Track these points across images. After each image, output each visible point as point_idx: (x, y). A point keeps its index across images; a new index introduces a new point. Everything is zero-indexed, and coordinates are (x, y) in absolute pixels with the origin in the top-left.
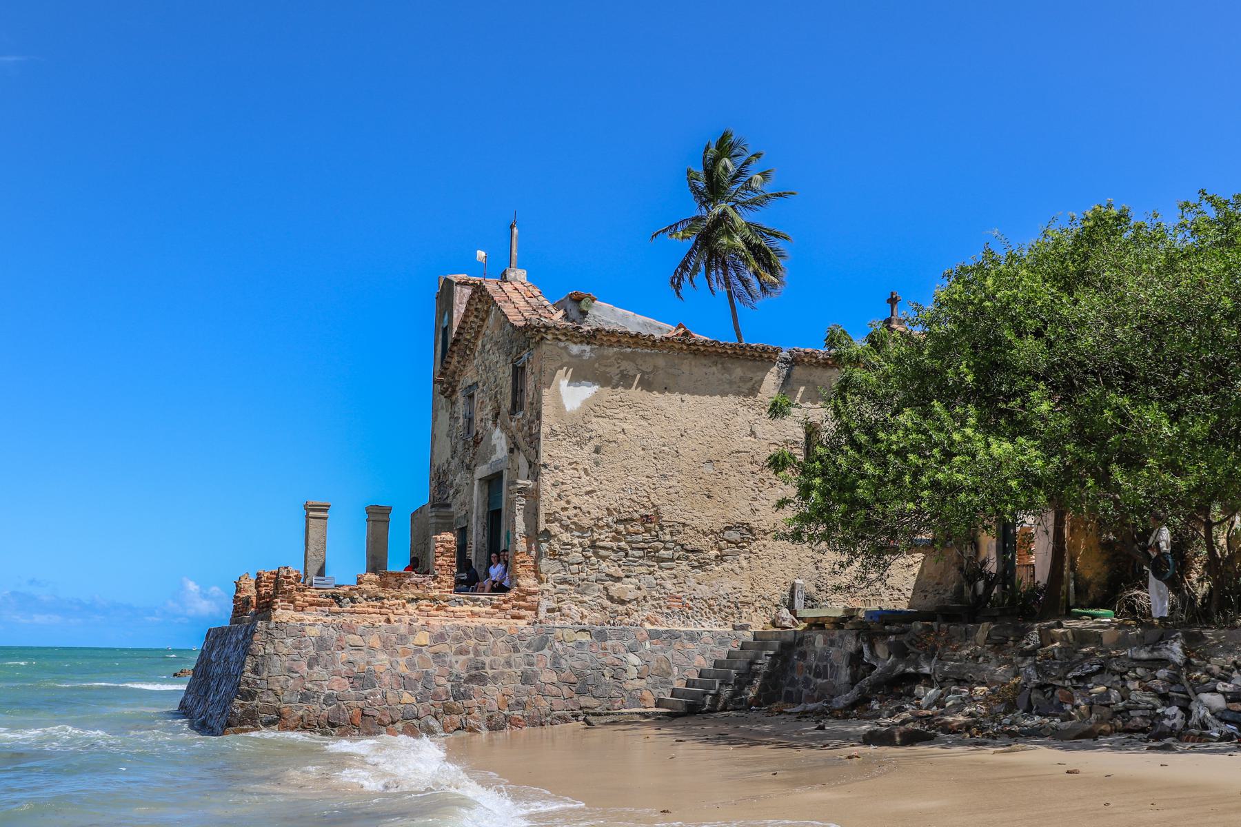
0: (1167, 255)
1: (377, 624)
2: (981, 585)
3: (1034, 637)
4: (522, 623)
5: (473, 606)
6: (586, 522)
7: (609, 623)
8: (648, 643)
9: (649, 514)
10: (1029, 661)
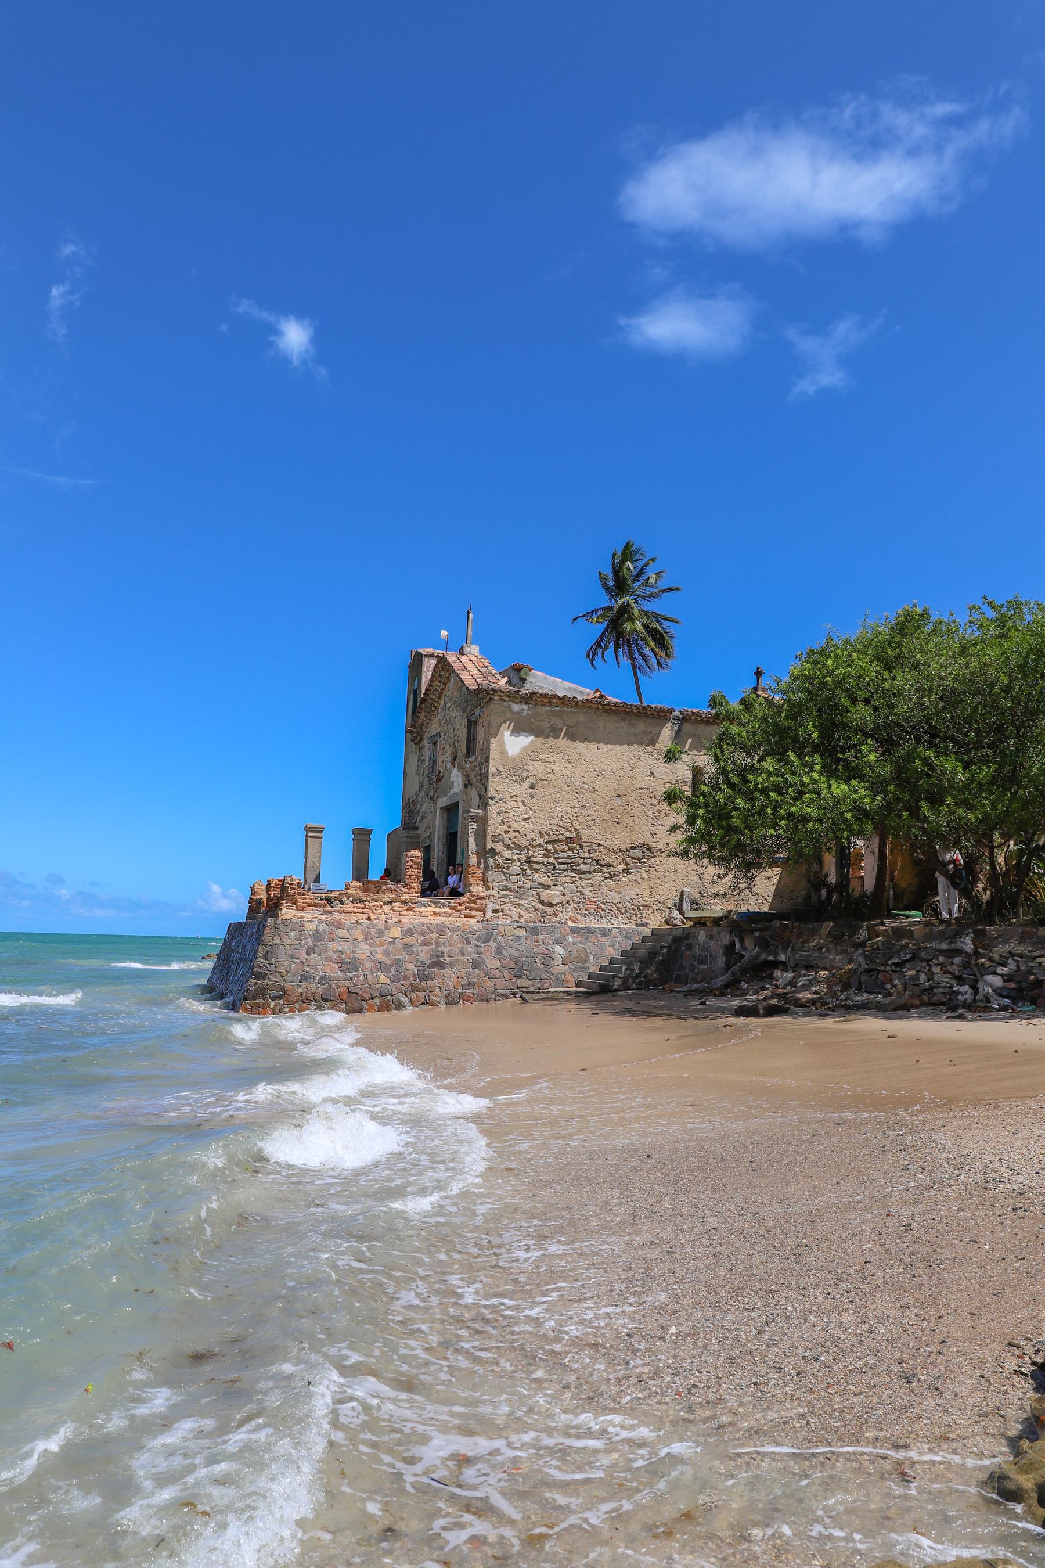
0: (961, 643)
1: (360, 921)
2: (824, 892)
3: (864, 933)
4: (473, 921)
5: (436, 907)
6: (523, 842)
7: (540, 921)
8: (570, 937)
10: (860, 951)
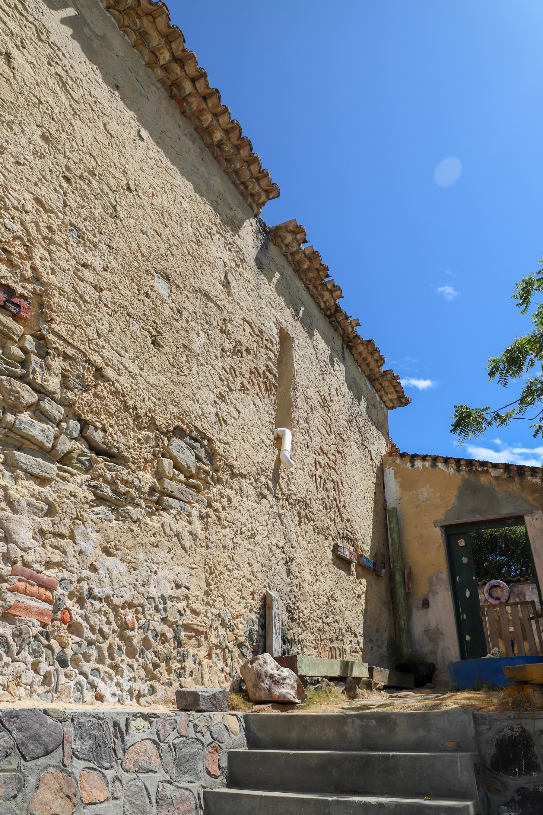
9: (20, 290)
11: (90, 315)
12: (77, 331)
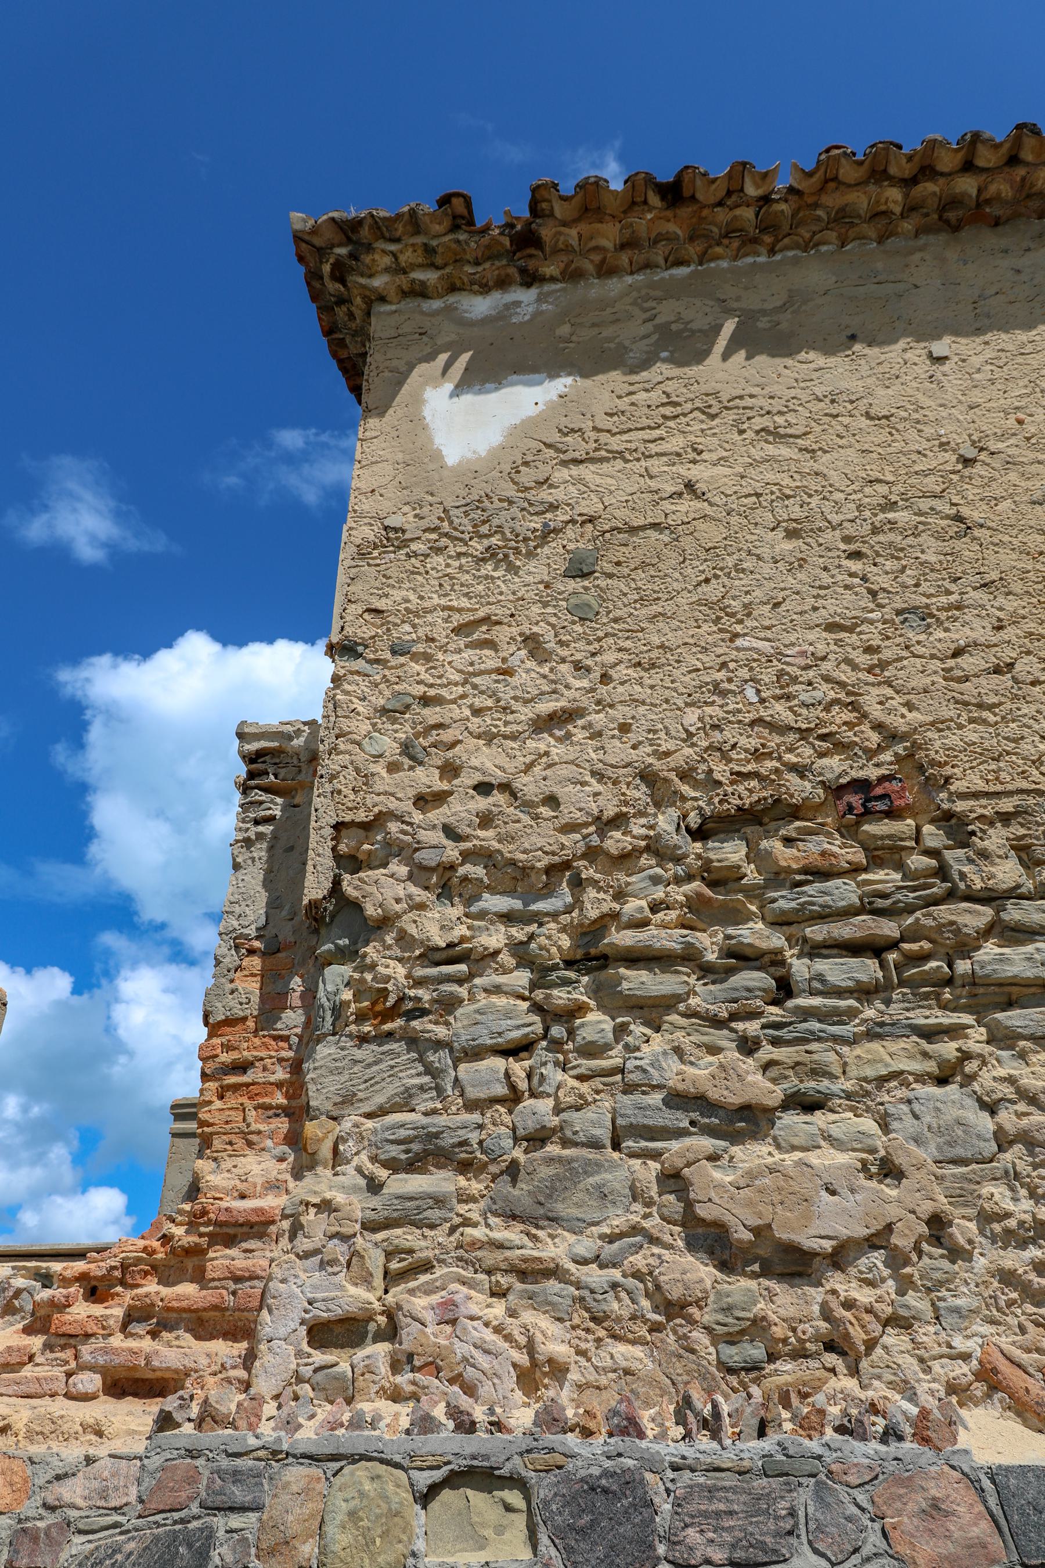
9: (873, 773)
11: (1013, 721)
12: (1001, 764)
